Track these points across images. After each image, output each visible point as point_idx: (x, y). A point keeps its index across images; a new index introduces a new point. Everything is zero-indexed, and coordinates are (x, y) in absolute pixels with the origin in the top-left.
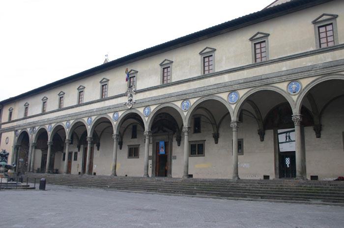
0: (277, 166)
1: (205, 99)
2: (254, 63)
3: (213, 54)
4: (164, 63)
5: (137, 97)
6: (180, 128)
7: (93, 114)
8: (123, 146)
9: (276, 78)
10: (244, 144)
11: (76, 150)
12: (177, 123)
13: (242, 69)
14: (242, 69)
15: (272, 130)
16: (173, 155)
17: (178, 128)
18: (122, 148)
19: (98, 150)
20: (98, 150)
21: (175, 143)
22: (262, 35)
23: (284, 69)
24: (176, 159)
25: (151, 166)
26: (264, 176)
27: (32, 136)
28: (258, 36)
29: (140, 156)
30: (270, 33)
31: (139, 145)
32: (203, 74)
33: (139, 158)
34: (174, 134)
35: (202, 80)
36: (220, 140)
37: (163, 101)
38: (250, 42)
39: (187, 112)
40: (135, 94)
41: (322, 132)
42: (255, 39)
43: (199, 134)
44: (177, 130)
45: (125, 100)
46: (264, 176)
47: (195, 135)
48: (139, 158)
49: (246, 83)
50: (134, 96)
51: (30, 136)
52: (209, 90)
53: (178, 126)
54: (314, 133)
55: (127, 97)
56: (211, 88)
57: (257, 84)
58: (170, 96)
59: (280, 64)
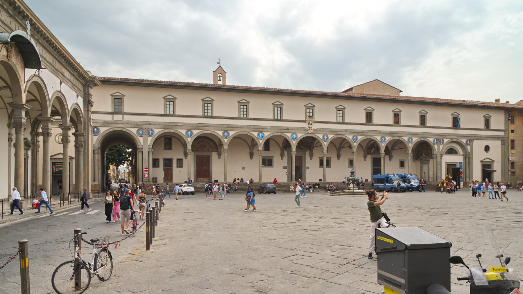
4: (338, 107)
7: (266, 130)
8: (254, 157)
11: (182, 157)
15: (370, 155)
19: (219, 157)
20: (219, 157)
21: (308, 157)
24: (309, 169)
25: (287, 174)
26: (366, 180)
27: (145, 141)
31: (274, 157)
40: (314, 123)
41: (392, 159)
42: (395, 111)
45: (305, 125)
46: (366, 180)
49: (391, 133)
51: (140, 140)
54: (389, 159)
58: (346, 131)
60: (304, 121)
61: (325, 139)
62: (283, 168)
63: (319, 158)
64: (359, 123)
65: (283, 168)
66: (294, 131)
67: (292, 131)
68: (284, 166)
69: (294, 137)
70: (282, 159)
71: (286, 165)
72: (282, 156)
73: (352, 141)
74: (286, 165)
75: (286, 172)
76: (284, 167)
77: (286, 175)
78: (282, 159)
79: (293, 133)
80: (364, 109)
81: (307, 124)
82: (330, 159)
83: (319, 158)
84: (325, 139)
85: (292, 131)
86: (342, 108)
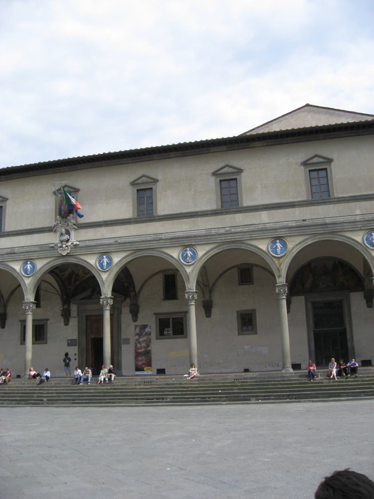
0: (313, 348)
1: (225, 247)
2: (310, 198)
3: (238, 177)
5: (75, 238)
6: (137, 290)
9: (348, 224)
10: (257, 318)
12: (133, 282)
13: (292, 205)
14: (292, 205)
16: (123, 336)
17: (135, 291)
18: (6, 326)
22: (322, 160)
23: (358, 212)
25: (77, 357)
28: (316, 160)
29: (48, 341)
30: (334, 159)
31: (48, 320)
32: (220, 207)
33: (46, 343)
34: (125, 300)
35: (220, 217)
36: (214, 311)
37: (143, 246)
38: (302, 168)
39: (191, 268)
40: (76, 229)
43: (175, 301)
44: (132, 294)
47: (167, 303)
48: (46, 343)
50: (73, 233)
52: (235, 233)
53: (134, 287)
55: (58, 234)
56: (239, 230)
57: (319, 230)
59: (352, 205)
60: (50, 230)
61: (105, 264)
62: (69, 345)
63: (155, 314)
64: (197, 212)
65: (69, 345)
66: (27, 256)
67: (22, 257)
68: (70, 340)
69: (29, 267)
70: (66, 324)
71: (75, 338)
72: (66, 316)
73: (178, 261)
74: (75, 336)
75: (75, 355)
76: (71, 343)
77: (75, 359)
78: (66, 324)
79: (26, 261)
80: (212, 170)
81: (58, 234)
82: (186, 316)
83: (155, 314)
84: (105, 264)
85: (22, 257)
86: (150, 182)
